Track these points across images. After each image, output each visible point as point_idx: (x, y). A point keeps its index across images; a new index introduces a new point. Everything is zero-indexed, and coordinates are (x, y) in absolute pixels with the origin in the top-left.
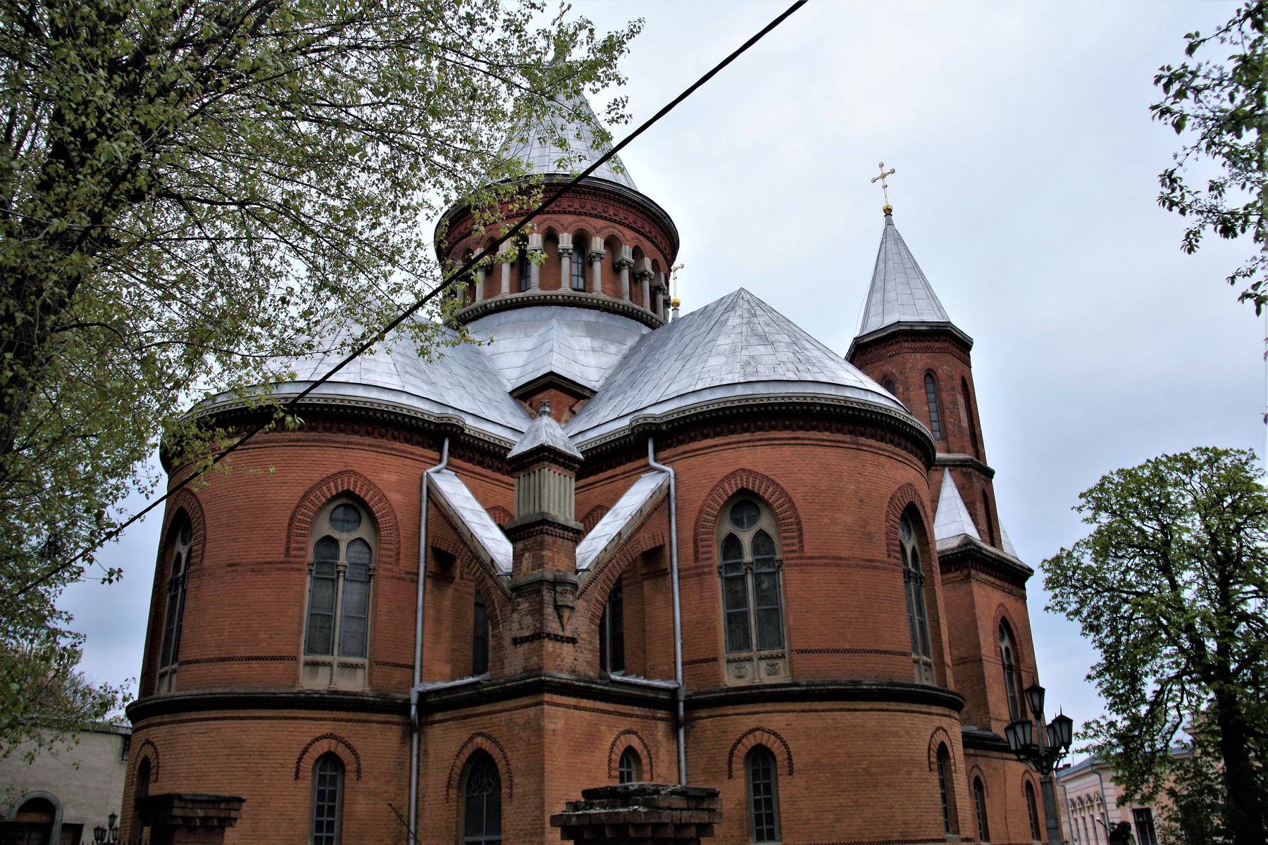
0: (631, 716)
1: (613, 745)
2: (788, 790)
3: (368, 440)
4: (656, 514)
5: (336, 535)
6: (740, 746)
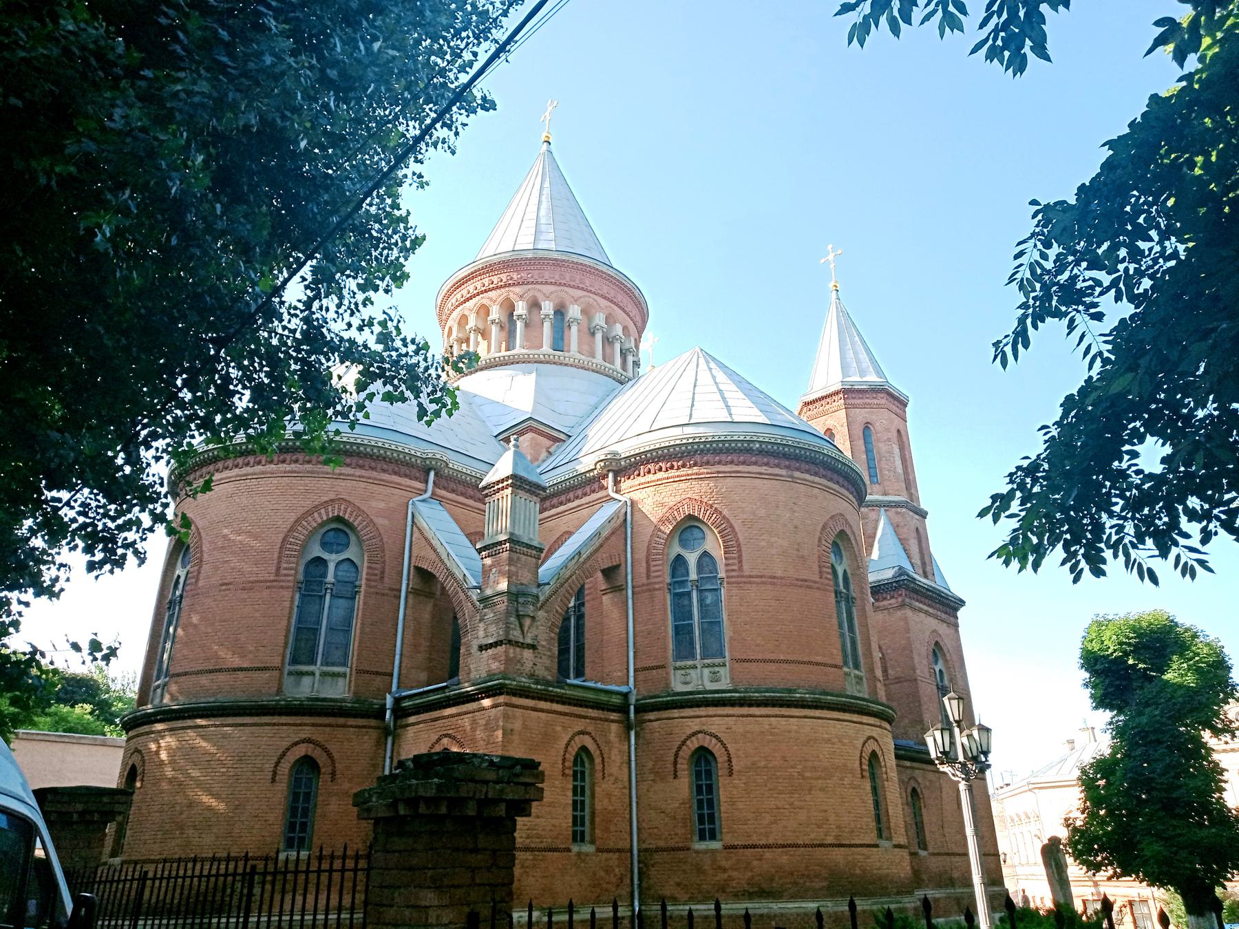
0: (585, 717)
1: (568, 745)
2: (727, 790)
3: (358, 472)
5: (325, 556)
6: (684, 747)
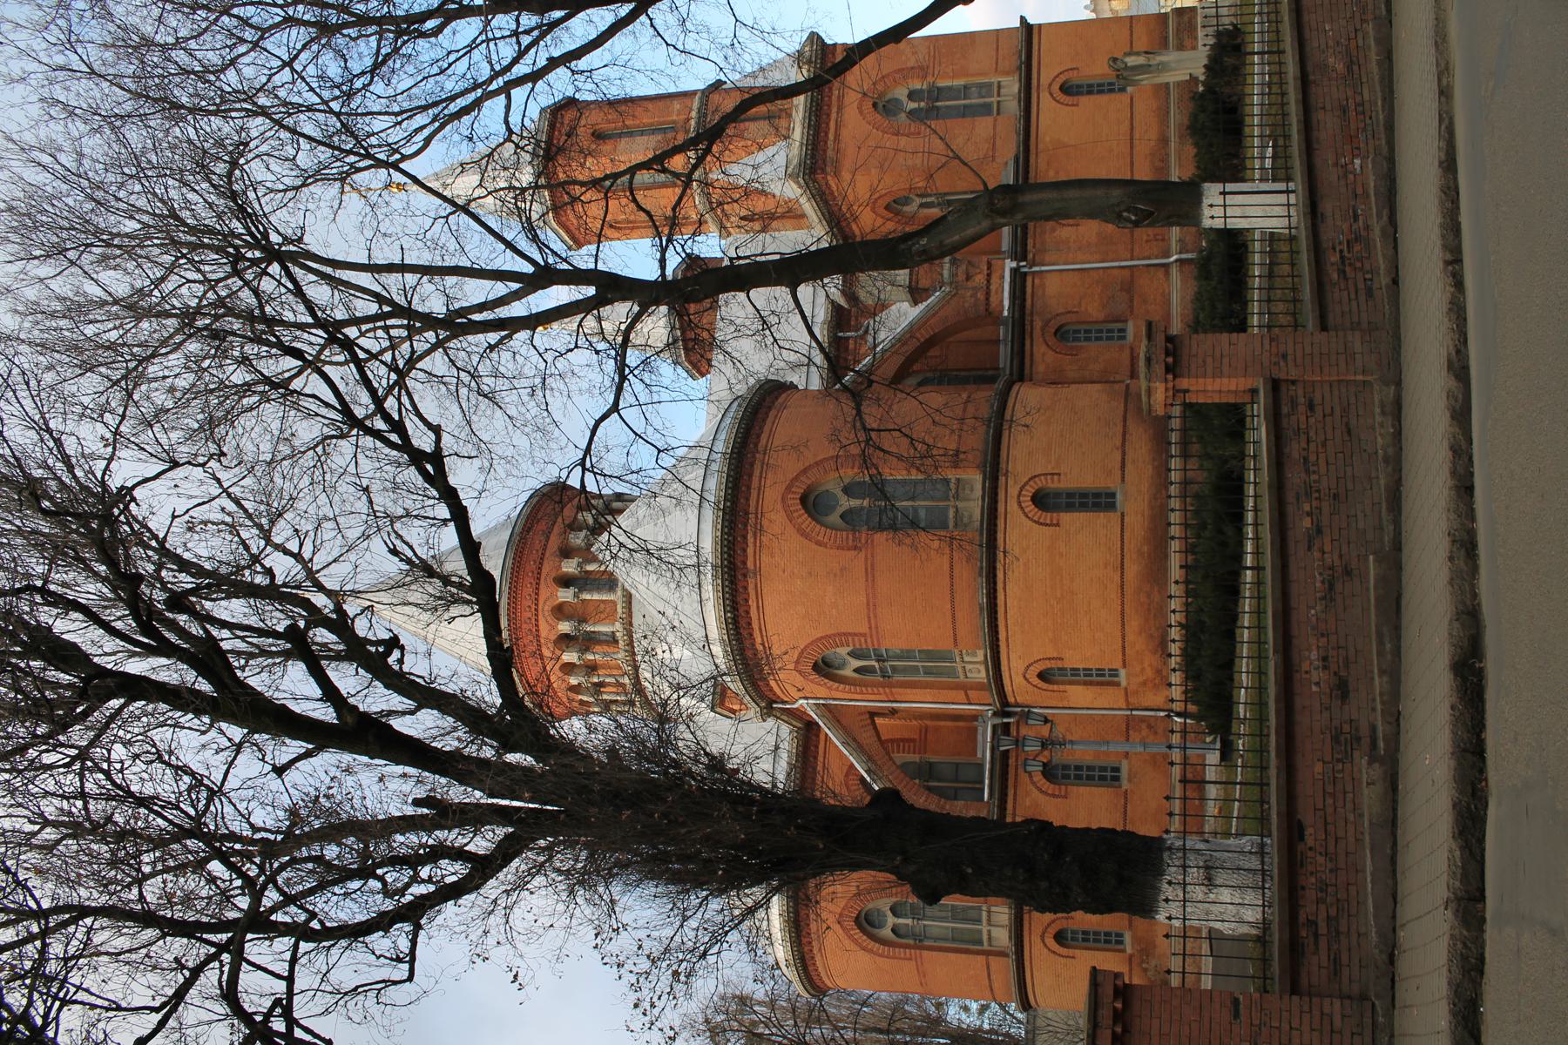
4: (844, 722)
